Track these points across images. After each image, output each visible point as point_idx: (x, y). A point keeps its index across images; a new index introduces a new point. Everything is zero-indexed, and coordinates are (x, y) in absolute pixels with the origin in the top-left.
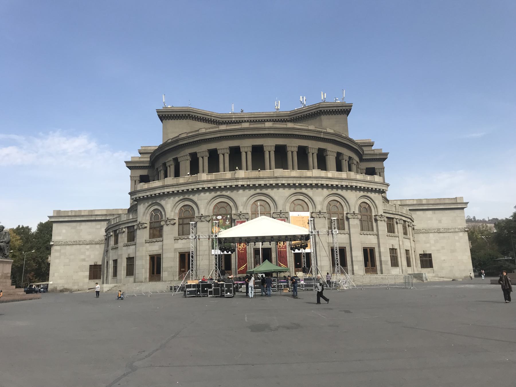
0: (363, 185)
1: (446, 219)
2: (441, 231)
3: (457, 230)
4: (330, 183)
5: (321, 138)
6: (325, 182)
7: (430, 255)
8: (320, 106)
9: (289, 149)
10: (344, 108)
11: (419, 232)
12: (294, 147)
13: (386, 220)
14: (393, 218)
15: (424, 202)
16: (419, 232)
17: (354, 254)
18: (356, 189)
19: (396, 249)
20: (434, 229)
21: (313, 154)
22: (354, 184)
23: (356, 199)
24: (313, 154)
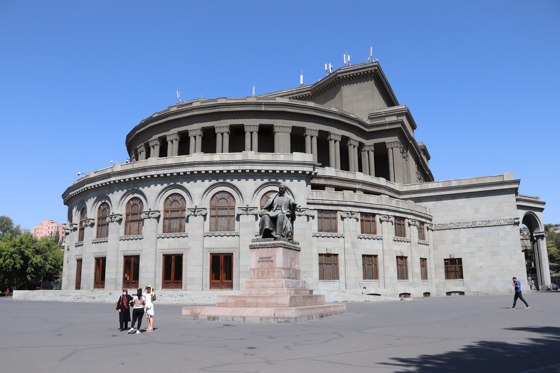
0: (264, 168)
1: (486, 208)
2: (477, 225)
3: (502, 222)
4: (210, 169)
5: (263, 111)
6: (203, 169)
7: (460, 260)
8: (338, 72)
9: (217, 131)
10: (367, 70)
11: (442, 228)
12: (223, 127)
13: (315, 213)
14: (336, 211)
15: (454, 184)
16: (442, 228)
17: (242, 262)
18: (258, 175)
19: (336, 255)
20: (466, 223)
21: (251, 133)
22: (248, 167)
23: (255, 188)
24: (251, 133)
